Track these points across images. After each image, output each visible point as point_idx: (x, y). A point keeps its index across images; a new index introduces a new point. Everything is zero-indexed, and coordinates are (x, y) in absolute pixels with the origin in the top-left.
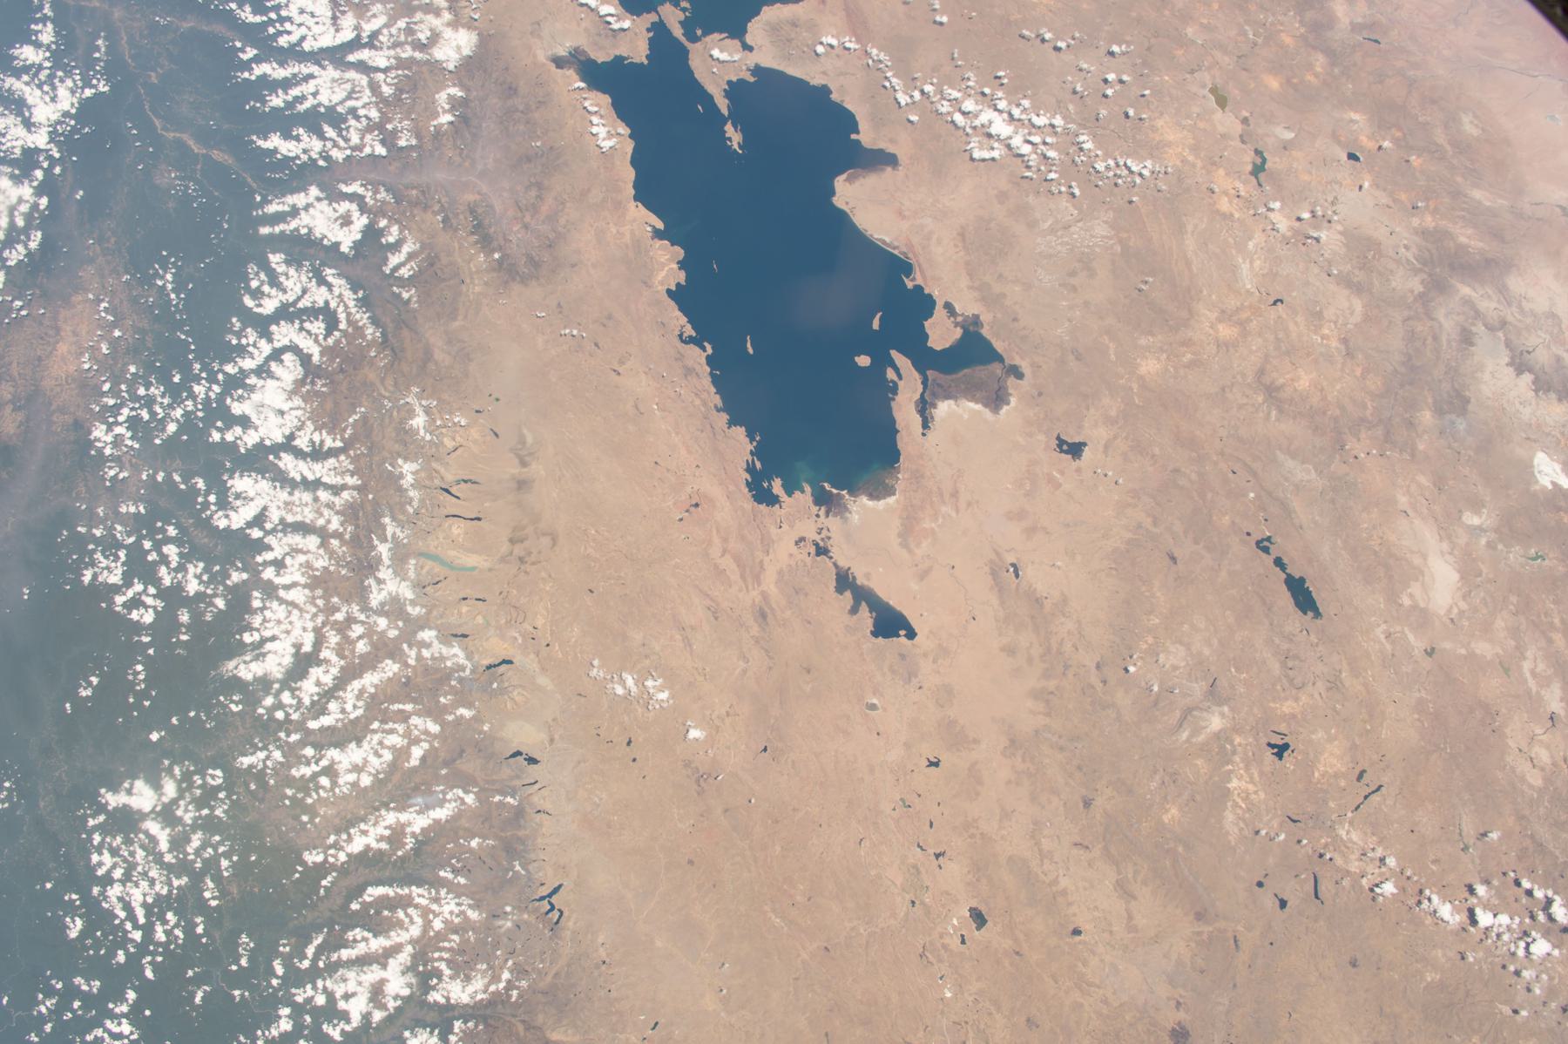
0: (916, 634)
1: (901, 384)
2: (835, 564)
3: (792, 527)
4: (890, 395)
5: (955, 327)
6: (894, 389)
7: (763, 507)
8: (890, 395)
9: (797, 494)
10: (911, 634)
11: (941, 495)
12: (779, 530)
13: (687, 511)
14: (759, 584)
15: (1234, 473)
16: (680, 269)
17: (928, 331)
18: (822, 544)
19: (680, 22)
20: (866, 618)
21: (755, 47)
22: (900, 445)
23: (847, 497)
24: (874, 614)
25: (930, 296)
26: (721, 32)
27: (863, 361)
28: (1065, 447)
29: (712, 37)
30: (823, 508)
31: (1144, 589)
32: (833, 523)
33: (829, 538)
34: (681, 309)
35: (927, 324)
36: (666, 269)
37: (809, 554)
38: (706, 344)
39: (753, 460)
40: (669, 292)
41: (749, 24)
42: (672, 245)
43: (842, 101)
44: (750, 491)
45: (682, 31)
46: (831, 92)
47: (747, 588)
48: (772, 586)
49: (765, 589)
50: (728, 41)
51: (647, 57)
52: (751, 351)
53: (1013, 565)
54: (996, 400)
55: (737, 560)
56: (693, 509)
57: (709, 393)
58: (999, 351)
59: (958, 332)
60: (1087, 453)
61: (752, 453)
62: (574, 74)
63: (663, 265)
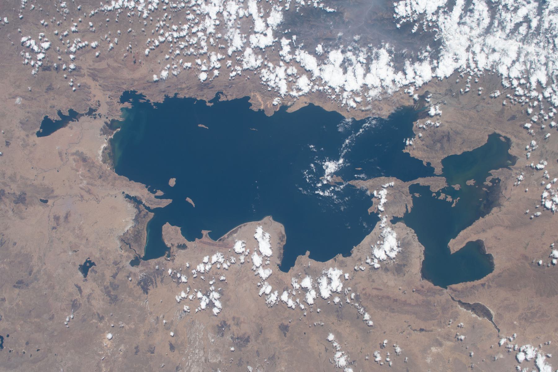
0: (38, 136)
1: (153, 196)
2: (82, 115)
3: (107, 103)
4: (149, 186)
5: (172, 244)
6: (151, 190)
7: (121, 93)
8: (149, 186)
9: (120, 113)
10: (39, 134)
11: (92, 185)
12: (108, 96)
13: (134, 57)
14: (88, 75)
15: (38, 350)
16: (260, 110)
17: (173, 227)
18: (94, 113)
19: (428, 187)
20: (55, 117)
21: (393, 225)
22: (122, 176)
23: (110, 137)
24: (54, 122)
25: (194, 240)
26: (412, 209)
27: (172, 182)
28: (88, 264)
29: (411, 202)
30: (109, 123)
31: (8, 260)
32: (100, 123)
33: (95, 118)
34: (236, 100)
35: (179, 229)
36: (262, 103)
37: (92, 105)
38: (212, 104)
39: (146, 100)
40: (249, 98)
41: (413, 231)
42: (275, 112)
43: (335, 259)
44: (131, 91)
45: (421, 184)
46: (344, 256)
47: (90, 69)
48: (85, 81)
49: (85, 77)
50: (404, 210)
51: (408, 154)
52: (200, 125)
53: (46, 202)
54: (125, 241)
55: (103, 70)
56: (134, 60)
57: (186, 94)
58: (149, 261)
59: (168, 244)
60: (80, 274)
61: (148, 101)
62: (409, 104)
63: (265, 102)
